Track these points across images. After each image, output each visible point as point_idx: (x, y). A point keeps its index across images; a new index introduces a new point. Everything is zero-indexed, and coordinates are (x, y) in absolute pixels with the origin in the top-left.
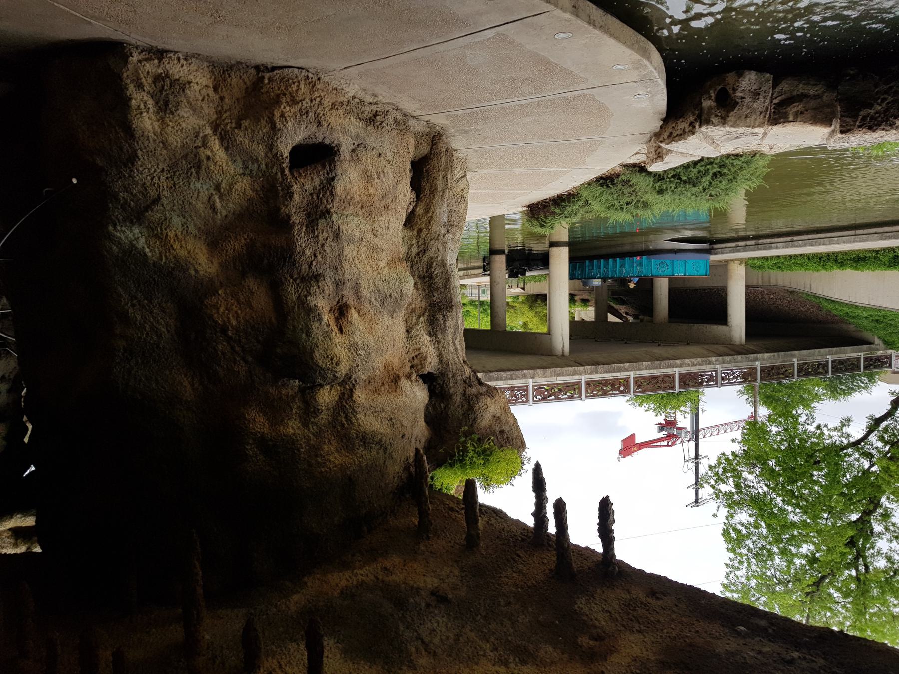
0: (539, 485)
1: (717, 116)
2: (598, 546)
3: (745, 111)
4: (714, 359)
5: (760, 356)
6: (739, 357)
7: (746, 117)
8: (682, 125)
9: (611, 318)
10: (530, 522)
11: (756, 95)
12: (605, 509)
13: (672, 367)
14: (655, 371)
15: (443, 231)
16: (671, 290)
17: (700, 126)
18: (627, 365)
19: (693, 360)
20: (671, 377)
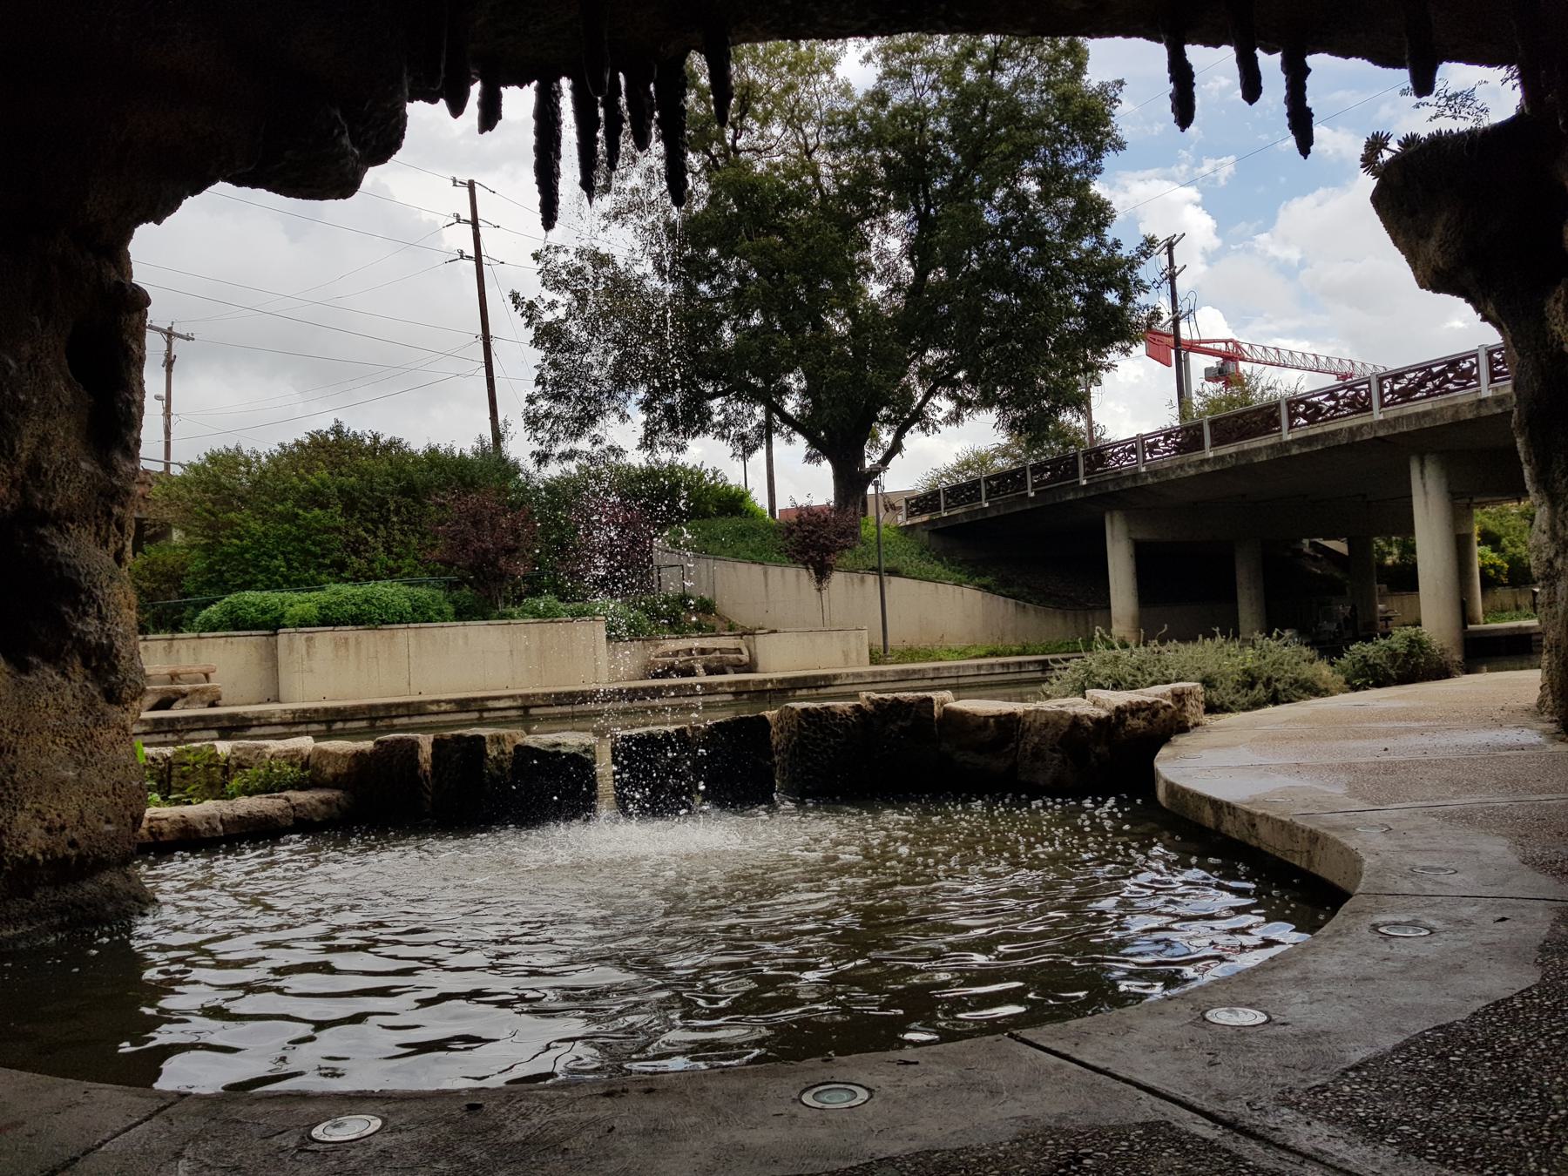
0: (1301, 122)
1: (1086, 729)
2: (1195, 54)
3: (1049, 733)
4: (1150, 480)
5: (1081, 495)
6: (1111, 488)
7: (1046, 725)
8: (1137, 723)
9: (1340, 546)
10: (1311, 60)
11: (1037, 754)
12: (1184, 110)
13: (1218, 459)
14: (1246, 447)
15: (1558, 563)
16: (1233, 600)
17: (1109, 718)
18: (1295, 451)
19: (1183, 474)
20: (1218, 441)
